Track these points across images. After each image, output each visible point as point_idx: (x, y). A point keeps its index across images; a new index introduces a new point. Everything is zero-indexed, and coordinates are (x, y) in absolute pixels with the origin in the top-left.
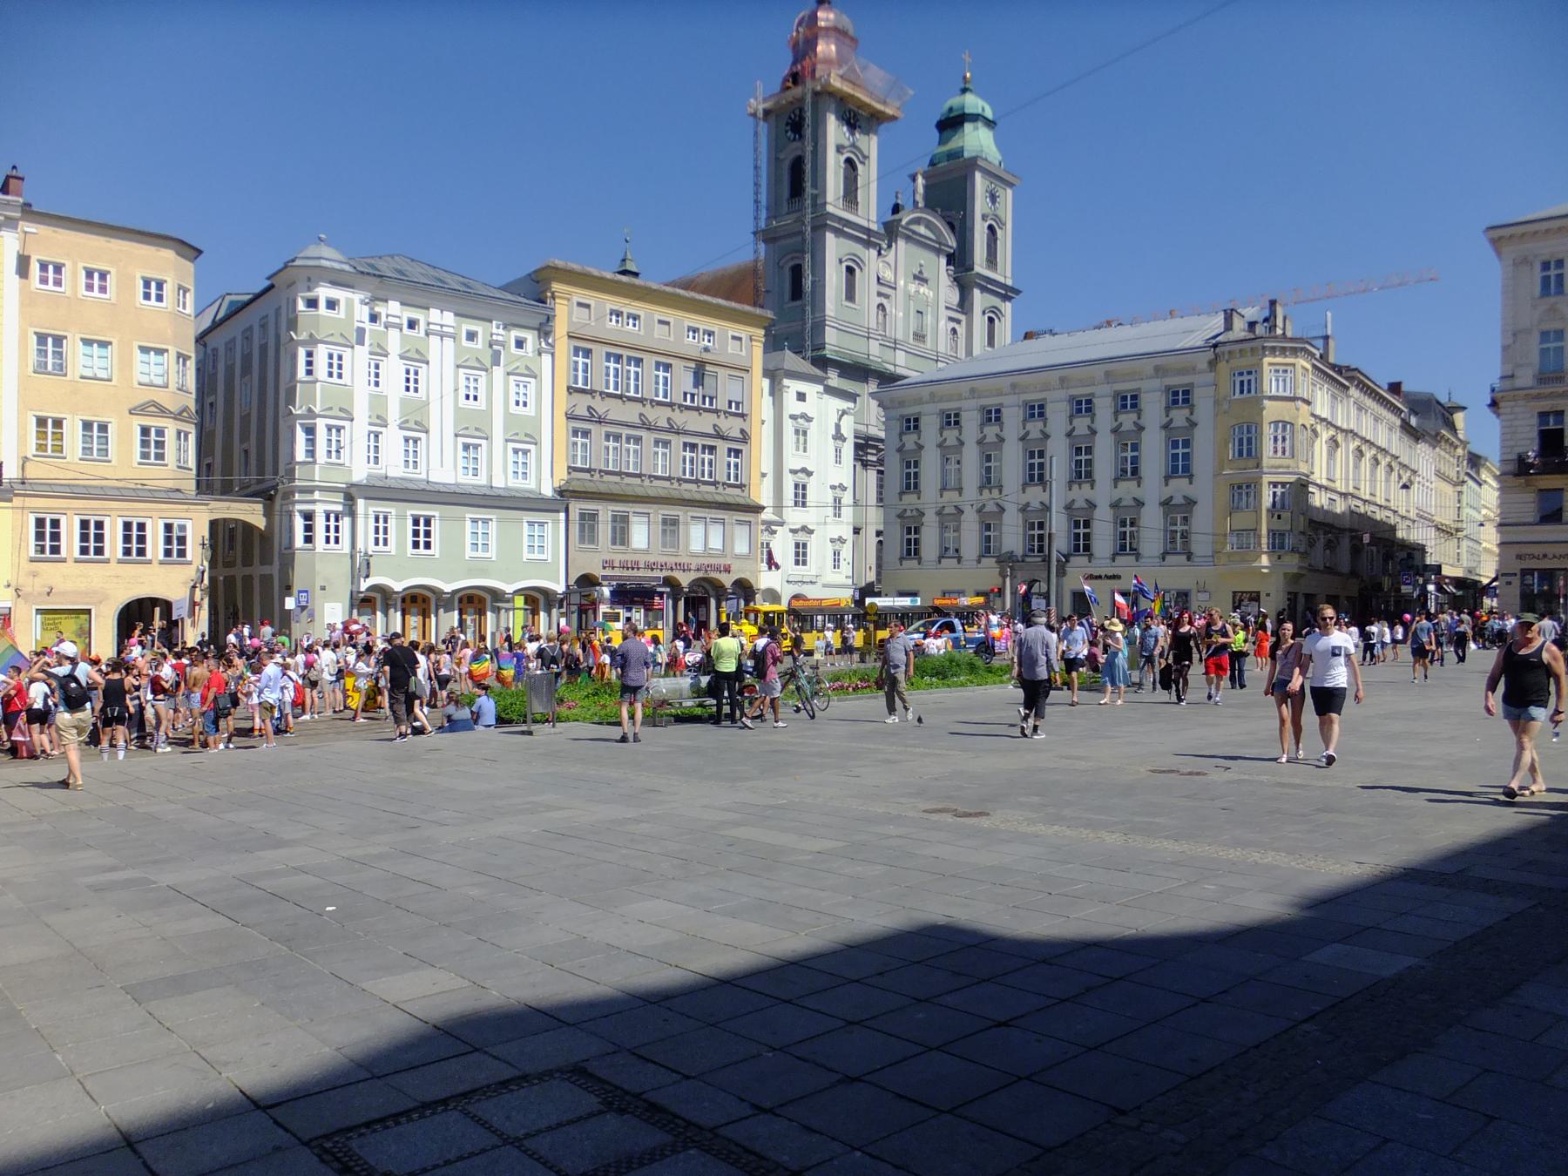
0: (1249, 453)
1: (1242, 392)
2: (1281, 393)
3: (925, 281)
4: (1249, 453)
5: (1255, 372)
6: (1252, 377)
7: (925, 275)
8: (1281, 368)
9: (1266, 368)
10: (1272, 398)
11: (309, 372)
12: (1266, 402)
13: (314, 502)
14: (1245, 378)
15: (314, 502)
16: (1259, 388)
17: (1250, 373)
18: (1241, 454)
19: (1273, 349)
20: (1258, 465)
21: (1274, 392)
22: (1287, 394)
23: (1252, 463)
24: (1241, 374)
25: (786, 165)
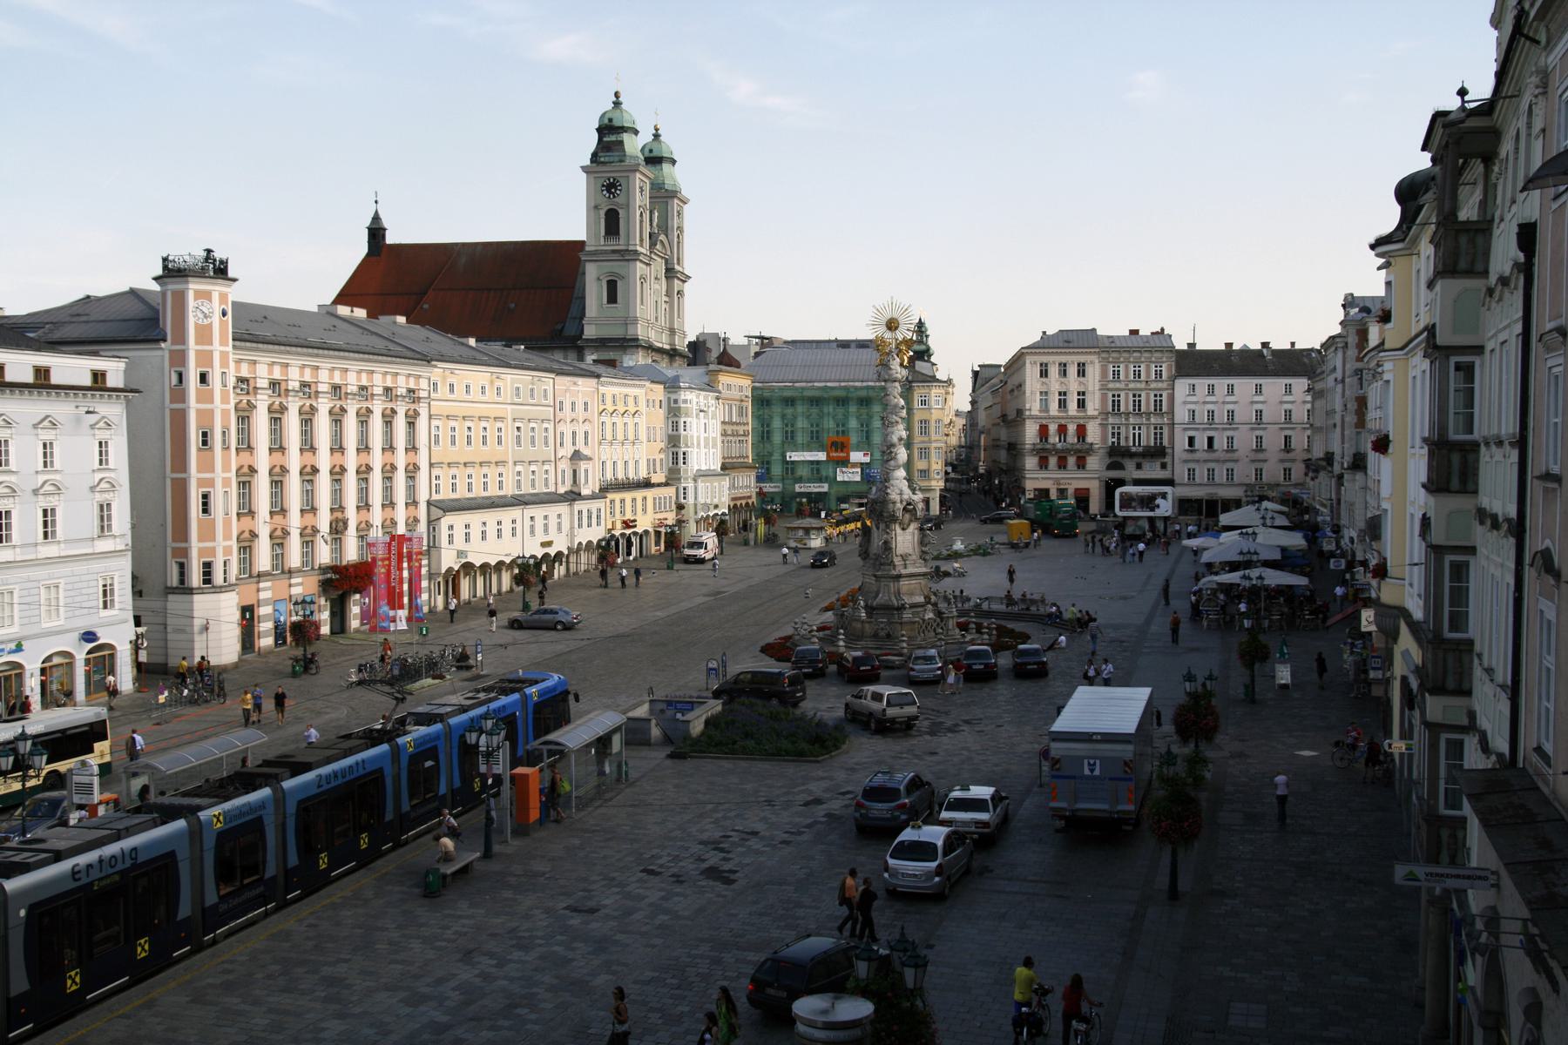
25: (602, 213)
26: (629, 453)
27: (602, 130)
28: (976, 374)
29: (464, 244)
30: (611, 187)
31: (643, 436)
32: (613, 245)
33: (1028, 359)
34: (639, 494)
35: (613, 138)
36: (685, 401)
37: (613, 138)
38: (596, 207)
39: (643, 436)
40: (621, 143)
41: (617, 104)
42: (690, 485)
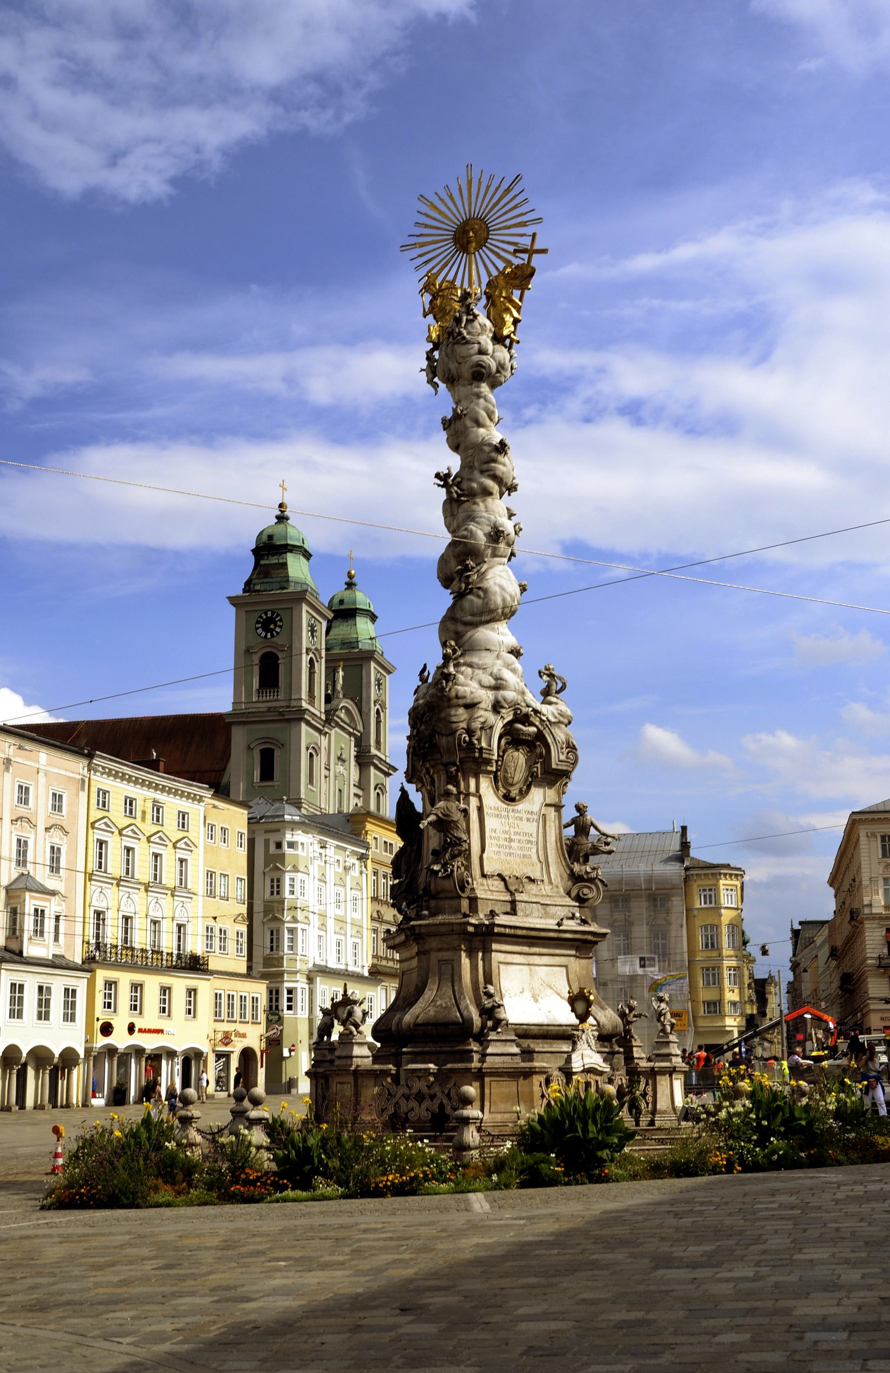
0: (713, 946)
1: (705, 903)
2: (730, 906)
3: (344, 761)
4: (713, 946)
5: (715, 889)
6: (713, 893)
7: (343, 757)
8: (730, 888)
9: (722, 887)
10: (726, 908)
11: (292, 892)
12: (723, 911)
13: (297, 981)
14: (708, 893)
15: (297, 981)
16: (717, 901)
17: (710, 890)
18: (707, 946)
19: (725, 875)
20: (720, 955)
21: (726, 905)
22: (733, 906)
23: (715, 954)
24: (704, 890)
25: (256, 659)
26: (165, 907)
27: (258, 552)
28: (796, 934)
29: (88, 723)
30: (268, 624)
31: (197, 881)
32: (271, 700)
33: (863, 832)
34: (180, 984)
35: (274, 560)
36: (291, 845)
37: (274, 560)
38: (248, 652)
39: (197, 881)
40: (284, 565)
41: (282, 519)
42: (301, 984)
